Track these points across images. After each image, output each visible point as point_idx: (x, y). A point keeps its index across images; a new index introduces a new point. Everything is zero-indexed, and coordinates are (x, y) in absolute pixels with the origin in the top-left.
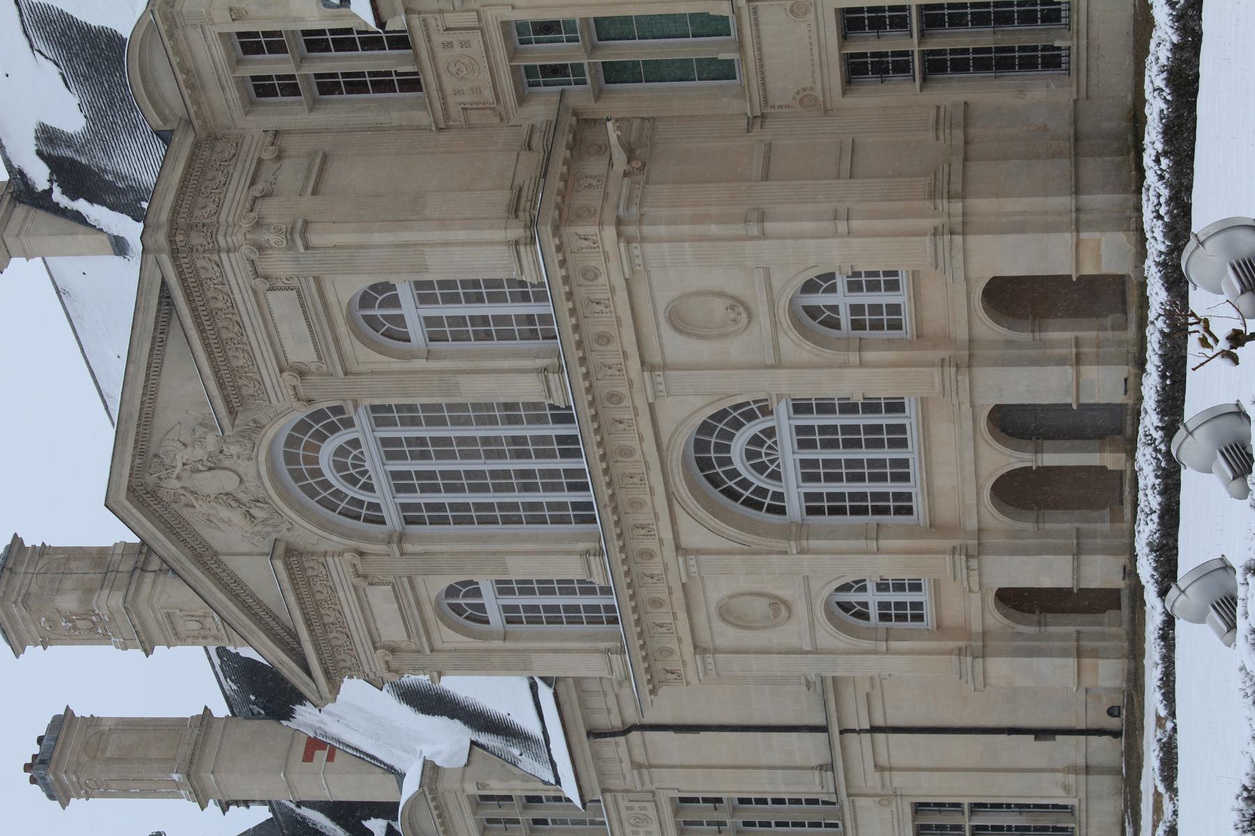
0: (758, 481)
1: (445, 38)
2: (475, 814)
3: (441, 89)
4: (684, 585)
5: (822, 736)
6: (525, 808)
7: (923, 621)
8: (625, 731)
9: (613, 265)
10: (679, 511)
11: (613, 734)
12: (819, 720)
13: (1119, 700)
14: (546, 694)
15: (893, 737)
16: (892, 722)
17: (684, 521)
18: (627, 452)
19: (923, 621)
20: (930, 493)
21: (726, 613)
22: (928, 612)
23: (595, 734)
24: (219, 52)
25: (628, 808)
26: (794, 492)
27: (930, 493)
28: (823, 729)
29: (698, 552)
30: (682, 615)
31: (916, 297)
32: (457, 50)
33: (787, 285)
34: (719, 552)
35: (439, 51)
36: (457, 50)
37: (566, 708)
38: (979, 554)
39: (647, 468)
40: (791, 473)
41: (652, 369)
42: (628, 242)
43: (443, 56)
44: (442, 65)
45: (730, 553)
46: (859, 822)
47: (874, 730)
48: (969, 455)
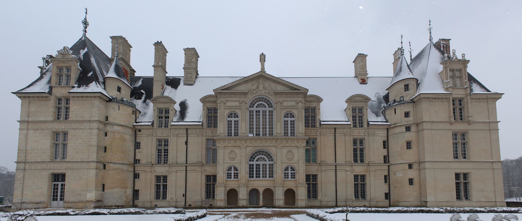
0: (256, 159)
1: (315, 131)
2: (164, 108)
3: (308, 129)
4: (240, 146)
7: (249, 178)
8: (187, 134)
9: (299, 145)
10: (254, 147)
11: (187, 132)
12: (188, 162)
13: (213, 206)
14: (200, 123)
17: (252, 148)
18: (266, 142)
19: (249, 178)
20: (254, 180)
21: (232, 151)
22: (251, 179)
23: (187, 129)
24: (314, 106)
25: (166, 132)
26: (255, 163)
27: (254, 180)
29: (246, 149)
30: (233, 145)
31: (290, 181)
32: (313, 132)
33: (295, 166)
34: (246, 152)
35: (314, 130)
36: (313, 132)
38: (247, 187)
39: (264, 144)
40: (258, 163)
41: (246, 147)
42: (281, 147)
43: (313, 131)
44: (312, 130)
45: (246, 153)
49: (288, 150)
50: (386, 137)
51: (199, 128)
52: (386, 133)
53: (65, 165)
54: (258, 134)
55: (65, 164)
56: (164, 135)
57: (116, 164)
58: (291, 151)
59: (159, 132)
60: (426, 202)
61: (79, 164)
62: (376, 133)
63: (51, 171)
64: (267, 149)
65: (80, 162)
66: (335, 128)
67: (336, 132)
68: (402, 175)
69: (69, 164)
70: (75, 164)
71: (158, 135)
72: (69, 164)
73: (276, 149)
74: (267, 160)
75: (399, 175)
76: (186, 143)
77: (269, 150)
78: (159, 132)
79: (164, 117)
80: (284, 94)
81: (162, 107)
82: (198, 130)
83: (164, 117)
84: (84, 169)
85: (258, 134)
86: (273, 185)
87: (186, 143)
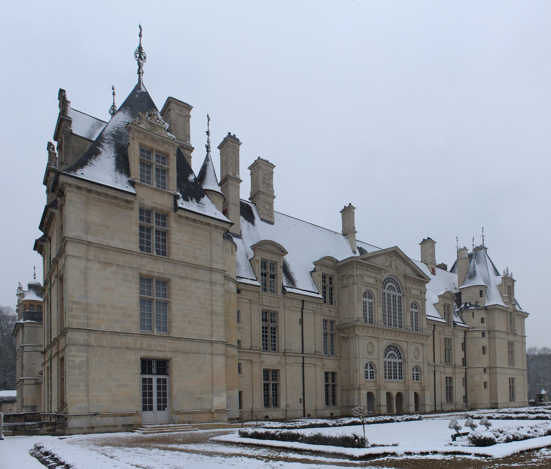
5: (301, 352)
6: (267, 273)
10: (389, 340)
12: (305, 352)
15: (301, 368)
16: (305, 368)
17: (388, 341)
28: (303, 353)
30: (371, 335)
37: (315, 299)
46: (272, 356)
47: (303, 364)
48: (396, 389)
49: (391, 343)
50: (463, 340)
51: (318, 302)
52: (464, 335)
53: (169, 344)
54: (390, 324)
55: (169, 341)
56: (273, 305)
57: (233, 348)
58: (418, 348)
59: (266, 299)
60: (497, 404)
61: (195, 343)
62: (459, 334)
63: (143, 354)
64: (399, 344)
65: (198, 341)
66: (435, 325)
67: (435, 330)
68: (479, 379)
69: (178, 344)
70: (188, 343)
71: (264, 304)
72: (177, 342)
73: (407, 345)
74: (397, 357)
75: (477, 378)
76: (301, 322)
77: (401, 345)
78: (266, 299)
79: (268, 276)
80: (374, 269)
81: (268, 258)
82: (315, 305)
83: (268, 276)
84: (204, 354)
85: (390, 324)
86: (404, 389)
87: (301, 322)
